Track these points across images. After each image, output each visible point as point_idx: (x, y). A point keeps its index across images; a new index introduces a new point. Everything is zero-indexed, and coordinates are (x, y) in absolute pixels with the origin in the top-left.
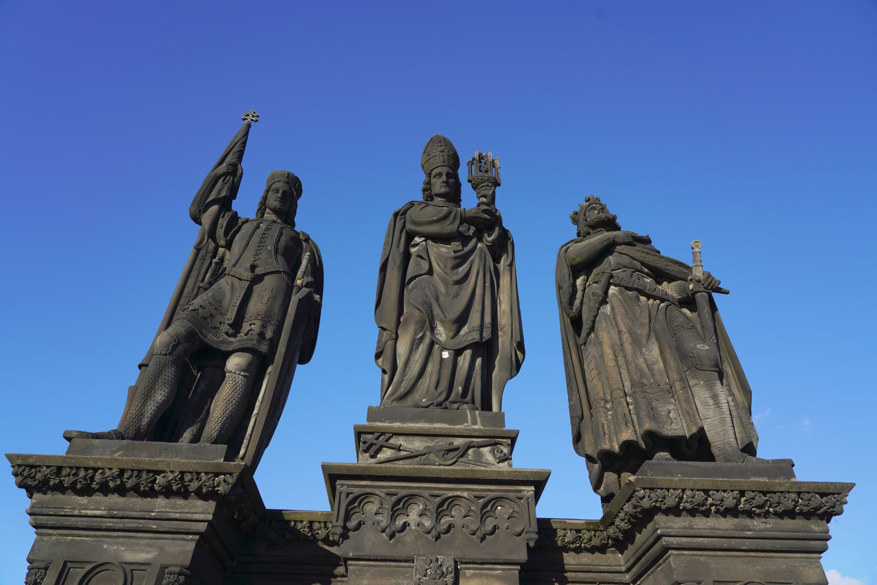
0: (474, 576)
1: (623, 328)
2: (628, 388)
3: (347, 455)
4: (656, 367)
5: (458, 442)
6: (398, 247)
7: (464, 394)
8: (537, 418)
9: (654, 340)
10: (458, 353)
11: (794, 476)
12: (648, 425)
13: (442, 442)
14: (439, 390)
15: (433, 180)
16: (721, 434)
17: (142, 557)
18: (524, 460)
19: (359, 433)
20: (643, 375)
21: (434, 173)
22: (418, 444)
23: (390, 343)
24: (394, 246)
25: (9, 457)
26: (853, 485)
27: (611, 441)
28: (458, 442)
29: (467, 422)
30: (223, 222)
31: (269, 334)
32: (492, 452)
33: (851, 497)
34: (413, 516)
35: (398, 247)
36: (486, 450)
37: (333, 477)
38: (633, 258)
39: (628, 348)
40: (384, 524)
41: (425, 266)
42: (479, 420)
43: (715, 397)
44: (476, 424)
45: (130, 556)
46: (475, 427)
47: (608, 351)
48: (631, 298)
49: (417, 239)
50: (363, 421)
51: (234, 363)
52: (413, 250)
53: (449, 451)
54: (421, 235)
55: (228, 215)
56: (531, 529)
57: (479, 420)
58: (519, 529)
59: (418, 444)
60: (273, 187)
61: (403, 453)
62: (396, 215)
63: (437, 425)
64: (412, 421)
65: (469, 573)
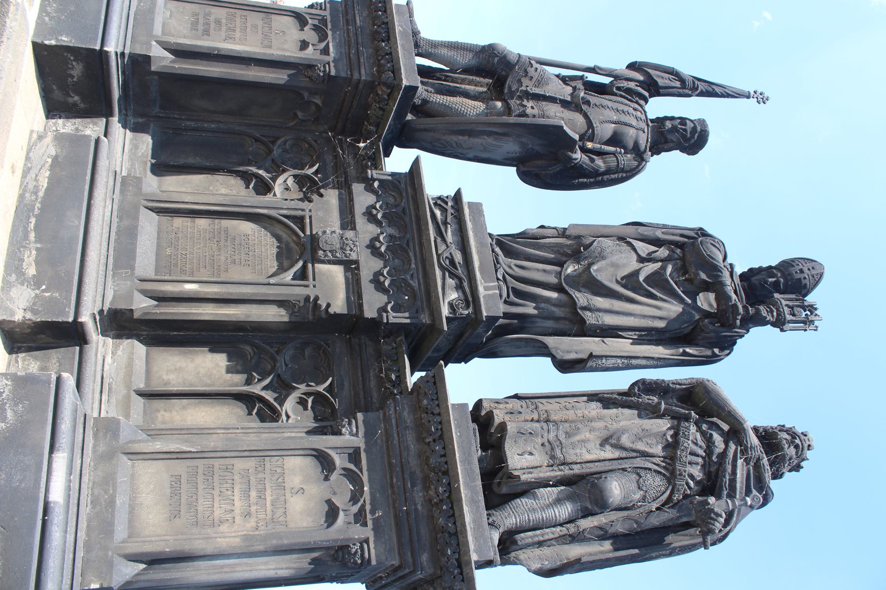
7: (518, 293)
9: (617, 454)
10: (559, 288)
12: (511, 428)
13: (458, 257)
19: (458, 197)
29: (485, 282)
42: (490, 292)
44: (486, 289)
46: (481, 289)
50: (466, 198)
53: (452, 262)
56: (391, 318)
57: (490, 292)
62: (701, 229)
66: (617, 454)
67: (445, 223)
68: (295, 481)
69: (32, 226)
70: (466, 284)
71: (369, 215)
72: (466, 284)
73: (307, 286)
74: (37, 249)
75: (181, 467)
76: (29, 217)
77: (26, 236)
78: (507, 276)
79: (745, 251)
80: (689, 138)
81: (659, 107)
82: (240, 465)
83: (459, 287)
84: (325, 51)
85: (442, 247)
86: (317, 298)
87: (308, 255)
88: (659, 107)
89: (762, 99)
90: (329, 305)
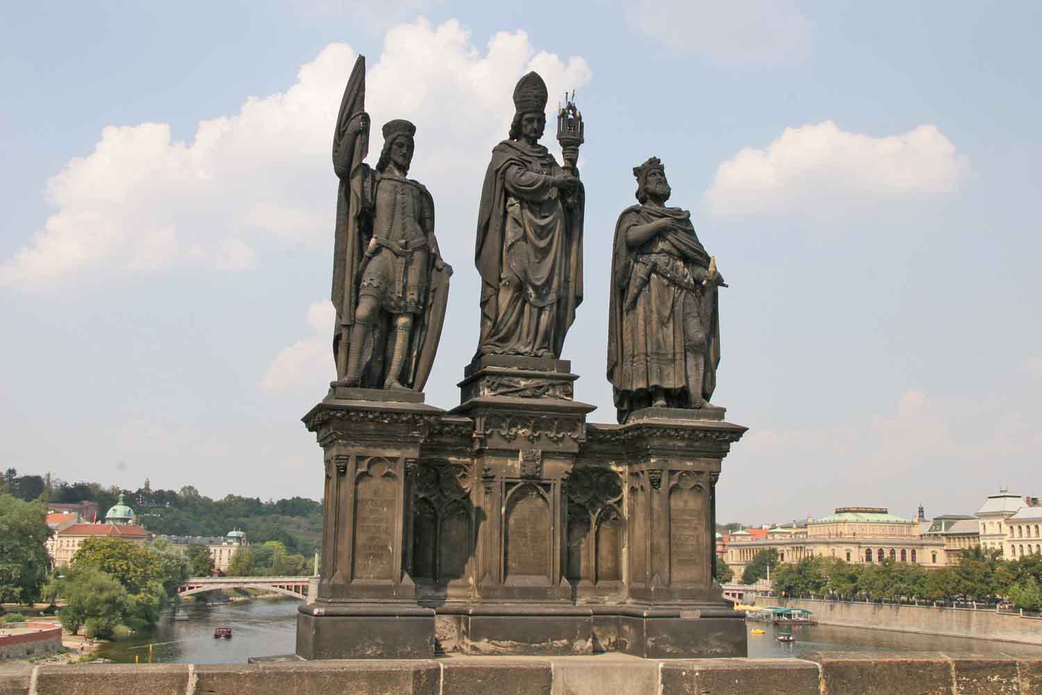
2: (649, 351)
4: (668, 340)
6: (499, 206)
8: (587, 344)
9: (671, 320)
10: (541, 310)
11: (723, 418)
16: (695, 389)
21: (527, 116)
23: (493, 298)
24: (496, 207)
26: (747, 429)
27: (632, 384)
30: (368, 184)
35: (499, 206)
38: (674, 246)
41: (521, 230)
43: (697, 366)
47: (641, 322)
48: (663, 284)
51: (402, 321)
52: (510, 209)
54: (516, 198)
55: (369, 179)
60: (398, 141)
66: (671, 320)
68: (681, 504)
69: (537, 645)
70: (554, 382)
71: (510, 439)
73: (555, 484)
74: (552, 640)
75: (674, 560)
76: (532, 648)
77: (544, 647)
78: (536, 347)
80: (401, 136)
82: (673, 531)
83: (553, 386)
84: (394, 460)
85: (528, 393)
86: (563, 479)
87: (534, 481)
90: (567, 472)
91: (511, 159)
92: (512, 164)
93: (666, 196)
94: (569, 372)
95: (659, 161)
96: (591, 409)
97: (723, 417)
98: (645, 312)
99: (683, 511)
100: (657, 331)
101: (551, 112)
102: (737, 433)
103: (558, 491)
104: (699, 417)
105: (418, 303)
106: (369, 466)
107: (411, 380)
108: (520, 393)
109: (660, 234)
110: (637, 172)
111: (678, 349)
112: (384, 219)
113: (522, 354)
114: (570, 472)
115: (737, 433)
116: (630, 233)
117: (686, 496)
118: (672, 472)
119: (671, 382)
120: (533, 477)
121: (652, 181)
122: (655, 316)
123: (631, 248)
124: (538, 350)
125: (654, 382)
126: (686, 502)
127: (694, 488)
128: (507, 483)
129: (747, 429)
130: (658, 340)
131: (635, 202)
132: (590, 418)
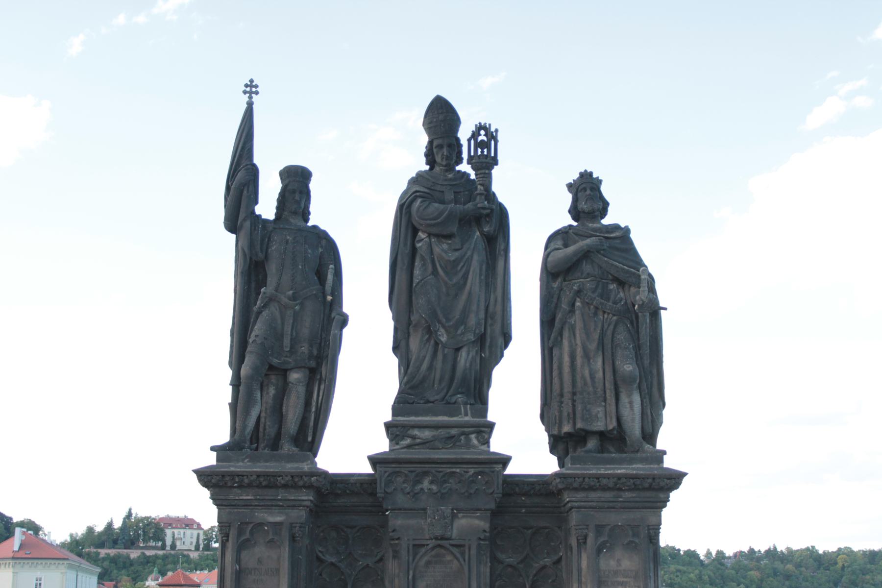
0: (463, 517)
1: (579, 342)
3: (382, 444)
4: (597, 376)
5: (454, 432)
6: (405, 244)
9: (600, 353)
14: (443, 385)
15: (435, 150)
17: (279, 519)
18: (497, 444)
20: (585, 384)
22: (427, 434)
24: (402, 245)
25: (195, 471)
28: (454, 432)
31: (315, 352)
32: (477, 438)
33: (685, 480)
34: (426, 484)
36: (473, 436)
37: (375, 461)
39: (579, 361)
40: (408, 490)
42: (469, 412)
44: (466, 415)
45: (272, 519)
46: (467, 418)
47: (566, 359)
49: (421, 235)
51: (294, 376)
52: (418, 245)
57: (469, 412)
58: (491, 491)
59: (427, 434)
61: (418, 441)
63: (440, 418)
64: (422, 415)
65: (460, 515)
67: (414, 437)
72: (466, 430)
78: (449, 394)
79: (410, 158)
81: (266, 207)
87: (445, 543)
88: (266, 207)
89: (251, 88)
90: (485, 531)
91: (416, 192)
92: (416, 196)
93: (604, 212)
94: (485, 416)
95: (591, 174)
96: (505, 461)
97: (662, 461)
98: (571, 346)
99: (616, 573)
100: (582, 366)
101: (464, 134)
102: (675, 479)
103: (474, 552)
104: (631, 461)
105: (311, 356)
106: (252, 533)
107: (310, 439)
108: (427, 445)
109: (586, 255)
110: (570, 186)
111: (607, 385)
112: (274, 271)
113: (433, 402)
114: (488, 530)
115: (675, 479)
116: (550, 259)
117: (619, 553)
118: (599, 529)
119: (599, 424)
120: (443, 538)
121: (587, 194)
122: (579, 351)
123: (554, 274)
124: (451, 396)
125: (579, 425)
126: (619, 561)
127: (628, 544)
128: (414, 545)
129: (685, 474)
130: (583, 377)
131: (567, 221)
132: (510, 470)
